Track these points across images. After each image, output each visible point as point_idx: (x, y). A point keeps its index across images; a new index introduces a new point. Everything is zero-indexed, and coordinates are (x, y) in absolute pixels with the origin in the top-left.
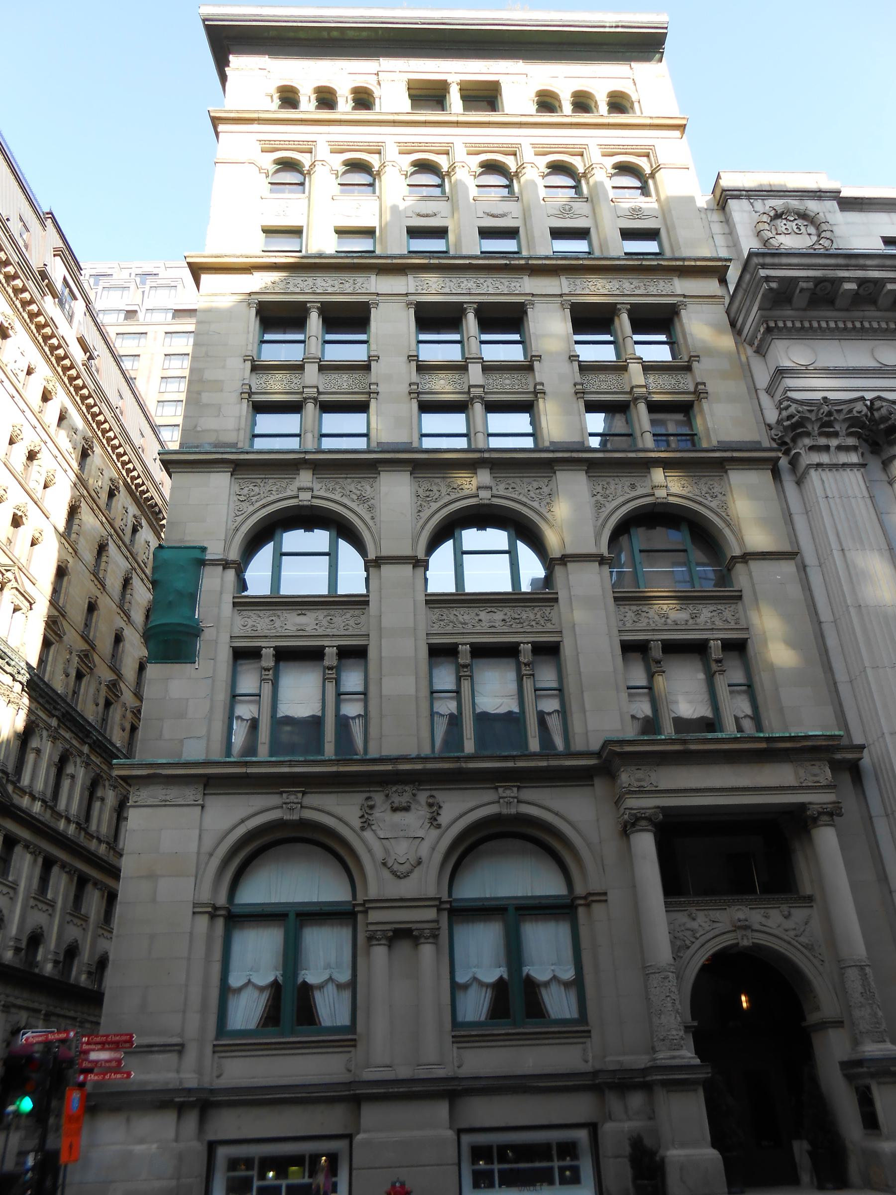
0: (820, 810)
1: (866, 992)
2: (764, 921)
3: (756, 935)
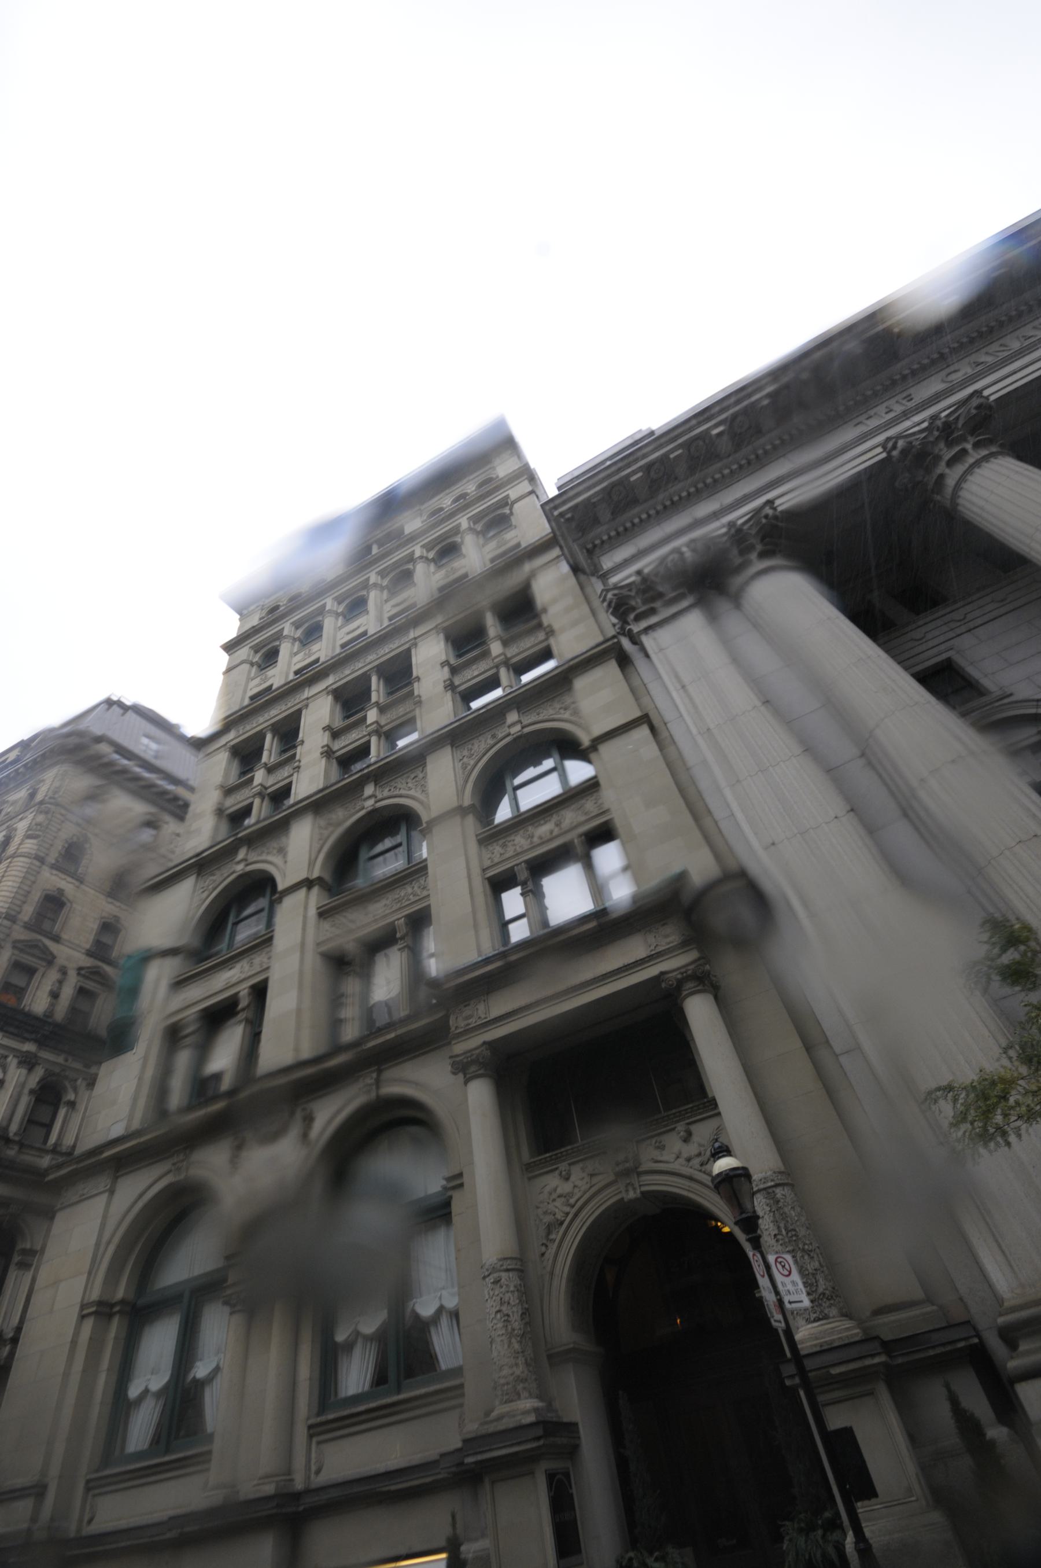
0: (679, 976)
1: (780, 1233)
2: (656, 1154)
3: (645, 1178)
